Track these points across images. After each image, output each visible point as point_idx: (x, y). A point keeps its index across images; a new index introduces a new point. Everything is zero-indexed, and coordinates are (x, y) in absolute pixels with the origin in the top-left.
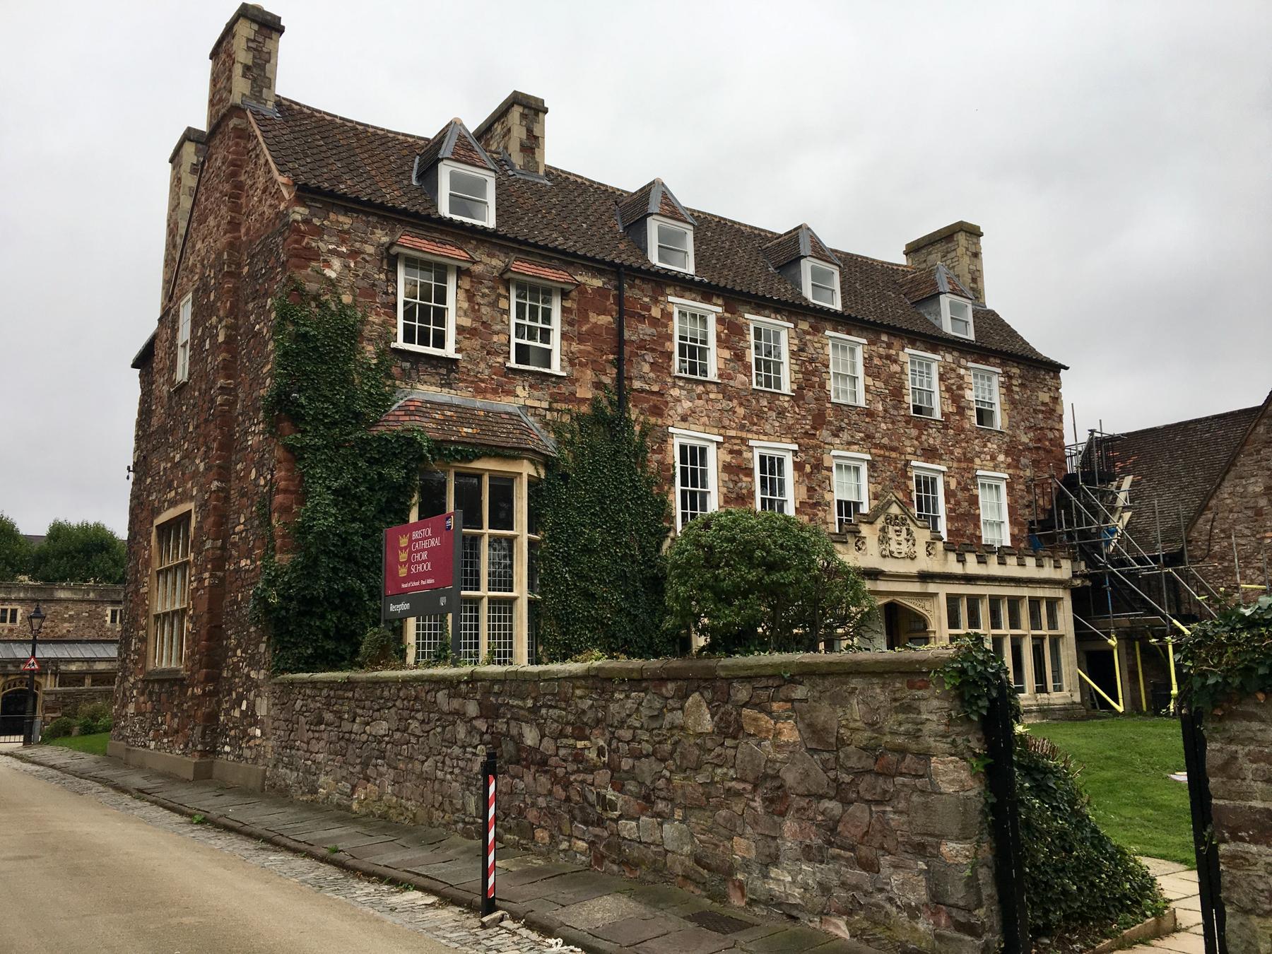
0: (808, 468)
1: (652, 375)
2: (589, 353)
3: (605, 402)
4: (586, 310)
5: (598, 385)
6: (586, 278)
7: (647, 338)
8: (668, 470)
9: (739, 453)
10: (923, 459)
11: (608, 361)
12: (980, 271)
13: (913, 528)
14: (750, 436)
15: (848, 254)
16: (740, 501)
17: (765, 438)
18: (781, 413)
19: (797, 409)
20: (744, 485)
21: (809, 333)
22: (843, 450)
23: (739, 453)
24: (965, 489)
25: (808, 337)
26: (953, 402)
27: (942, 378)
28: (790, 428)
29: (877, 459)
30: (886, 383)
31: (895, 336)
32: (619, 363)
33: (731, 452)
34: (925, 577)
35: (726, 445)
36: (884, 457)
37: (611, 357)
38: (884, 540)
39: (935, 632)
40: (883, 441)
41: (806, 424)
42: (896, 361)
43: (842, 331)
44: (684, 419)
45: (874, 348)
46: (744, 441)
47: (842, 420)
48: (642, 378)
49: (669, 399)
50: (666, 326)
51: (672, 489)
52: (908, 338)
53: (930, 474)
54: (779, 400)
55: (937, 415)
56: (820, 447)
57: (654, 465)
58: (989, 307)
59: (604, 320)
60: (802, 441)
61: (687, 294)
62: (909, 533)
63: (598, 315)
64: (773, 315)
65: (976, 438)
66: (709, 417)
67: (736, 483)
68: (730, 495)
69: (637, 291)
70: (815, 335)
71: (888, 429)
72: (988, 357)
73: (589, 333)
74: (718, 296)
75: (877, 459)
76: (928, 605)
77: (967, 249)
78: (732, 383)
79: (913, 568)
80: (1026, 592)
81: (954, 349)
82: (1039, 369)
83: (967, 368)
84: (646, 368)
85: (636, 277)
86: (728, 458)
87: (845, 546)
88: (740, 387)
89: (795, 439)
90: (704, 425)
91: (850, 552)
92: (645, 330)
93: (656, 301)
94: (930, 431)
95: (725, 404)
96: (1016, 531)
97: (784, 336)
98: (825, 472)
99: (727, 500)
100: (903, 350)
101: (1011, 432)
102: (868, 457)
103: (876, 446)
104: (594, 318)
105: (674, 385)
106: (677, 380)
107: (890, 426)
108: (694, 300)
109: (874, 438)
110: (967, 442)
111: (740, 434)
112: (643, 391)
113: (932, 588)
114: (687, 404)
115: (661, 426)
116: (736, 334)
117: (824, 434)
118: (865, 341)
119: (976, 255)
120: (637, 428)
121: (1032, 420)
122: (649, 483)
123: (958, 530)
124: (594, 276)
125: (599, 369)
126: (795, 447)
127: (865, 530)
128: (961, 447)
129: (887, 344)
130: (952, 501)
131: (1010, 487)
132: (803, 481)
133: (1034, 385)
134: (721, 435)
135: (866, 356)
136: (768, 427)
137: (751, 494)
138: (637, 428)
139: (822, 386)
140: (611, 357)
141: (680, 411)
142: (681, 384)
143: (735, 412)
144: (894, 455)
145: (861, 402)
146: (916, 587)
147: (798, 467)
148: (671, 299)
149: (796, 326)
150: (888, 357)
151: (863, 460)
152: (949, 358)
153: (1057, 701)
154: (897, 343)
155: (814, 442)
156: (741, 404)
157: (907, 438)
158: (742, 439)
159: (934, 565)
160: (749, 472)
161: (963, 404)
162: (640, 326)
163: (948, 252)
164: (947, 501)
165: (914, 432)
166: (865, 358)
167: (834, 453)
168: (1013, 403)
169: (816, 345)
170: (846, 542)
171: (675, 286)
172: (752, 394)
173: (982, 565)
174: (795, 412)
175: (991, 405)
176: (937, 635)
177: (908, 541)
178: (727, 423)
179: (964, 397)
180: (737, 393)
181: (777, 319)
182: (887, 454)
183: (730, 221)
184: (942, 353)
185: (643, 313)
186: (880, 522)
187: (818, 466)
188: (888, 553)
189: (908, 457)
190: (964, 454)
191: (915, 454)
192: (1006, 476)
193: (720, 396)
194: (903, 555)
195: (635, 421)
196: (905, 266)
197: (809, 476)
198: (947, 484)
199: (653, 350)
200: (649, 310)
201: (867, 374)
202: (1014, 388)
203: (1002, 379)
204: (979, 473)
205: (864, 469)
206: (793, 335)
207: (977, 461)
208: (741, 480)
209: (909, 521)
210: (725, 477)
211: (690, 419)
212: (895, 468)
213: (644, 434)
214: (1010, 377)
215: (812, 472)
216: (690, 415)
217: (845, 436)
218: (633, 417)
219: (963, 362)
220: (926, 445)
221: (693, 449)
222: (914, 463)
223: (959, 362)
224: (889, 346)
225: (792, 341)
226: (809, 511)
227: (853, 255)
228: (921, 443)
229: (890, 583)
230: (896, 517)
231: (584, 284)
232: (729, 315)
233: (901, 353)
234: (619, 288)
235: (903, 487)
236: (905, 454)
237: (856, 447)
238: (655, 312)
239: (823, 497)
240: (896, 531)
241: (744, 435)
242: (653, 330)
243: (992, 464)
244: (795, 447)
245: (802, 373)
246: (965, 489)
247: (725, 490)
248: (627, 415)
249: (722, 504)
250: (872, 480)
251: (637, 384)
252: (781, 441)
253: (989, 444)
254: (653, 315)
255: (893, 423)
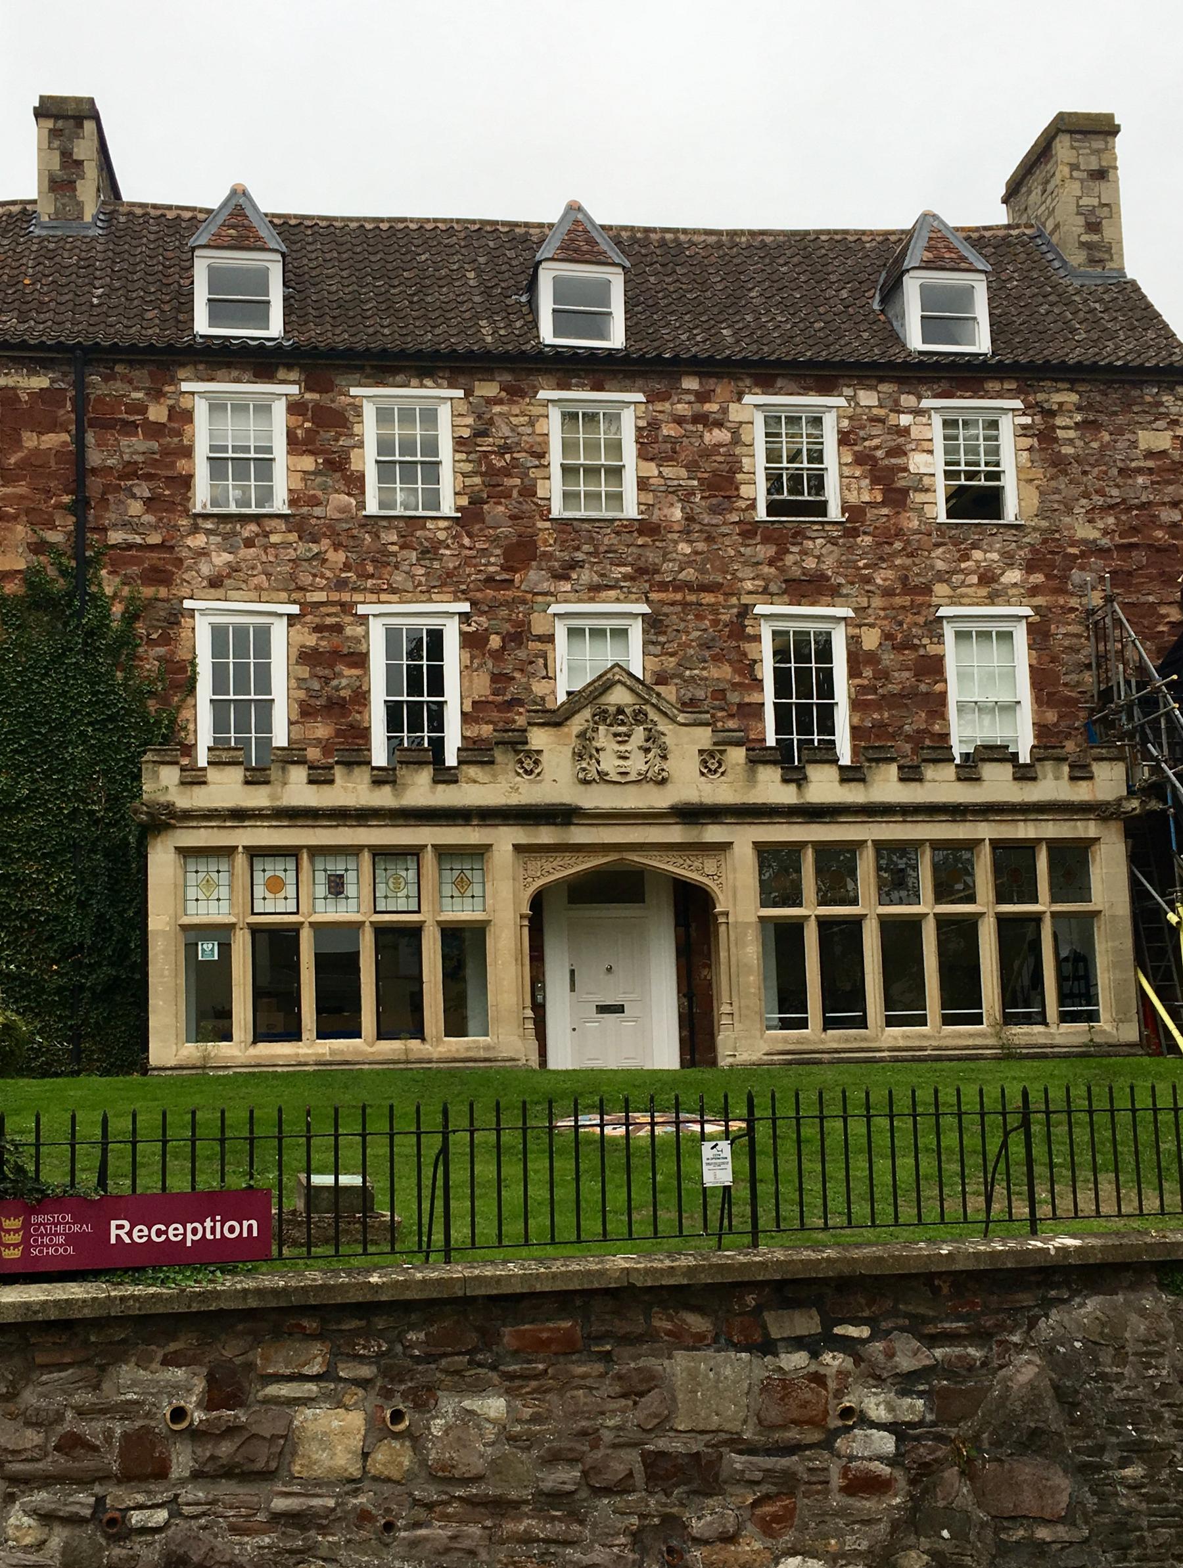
0: (495, 642)
1: (149, 518)
2: (22, 497)
3: (52, 572)
4: (17, 431)
5: (39, 547)
6: (16, 378)
7: (140, 459)
8: (183, 670)
9: (338, 628)
10: (786, 598)
11: (59, 506)
12: (1111, 208)
13: (663, 726)
14: (358, 597)
15: (794, 233)
16: (337, 710)
17: (395, 598)
18: (430, 551)
19: (466, 541)
20: (344, 682)
21: (499, 401)
22: (580, 601)
23: (338, 628)
24: (907, 645)
25: (497, 409)
26: (875, 481)
27: (844, 439)
28: (449, 575)
29: (666, 609)
30: (692, 467)
31: (719, 376)
32: (80, 507)
33: (318, 629)
34: (690, 814)
35: (309, 618)
36: (685, 604)
37: (66, 499)
38: (585, 751)
39: (727, 914)
40: (681, 576)
41: (489, 564)
42: (719, 424)
43: (581, 386)
44: (215, 583)
45: (659, 406)
46: (347, 608)
47: (578, 549)
48: (128, 525)
49: (184, 553)
50: (179, 433)
51: (190, 701)
52: (750, 375)
53: (812, 627)
54: (424, 528)
55: (834, 512)
56: (524, 602)
57: (150, 666)
58: (1130, 276)
59: (53, 440)
60: (479, 595)
61: (219, 374)
62: (652, 737)
63: (40, 433)
64: (414, 382)
65: (938, 545)
66: (268, 575)
67: (327, 680)
68: (312, 702)
69: (119, 384)
70: (512, 402)
71: (696, 553)
72: (982, 381)
73: (22, 465)
74: (289, 367)
75: (666, 609)
76: (710, 866)
77: (1074, 167)
78: (318, 511)
79: (661, 799)
80: (985, 831)
81: (882, 380)
82: (1139, 384)
83: (917, 412)
84: (135, 508)
85: (116, 362)
86: (311, 640)
87: (487, 768)
88: (337, 516)
89: (463, 592)
90: (259, 588)
91: (501, 778)
92: (136, 446)
93: (157, 394)
94: (810, 544)
95: (303, 549)
96: (1051, 716)
97: (444, 414)
98: (534, 646)
99: (305, 712)
100: (739, 400)
101: (1044, 524)
102: (645, 608)
103: (663, 587)
104: (30, 440)
105: (195, 530)
106: (200, 521)
107: (701, 546)
108: (237, 380)
109: (657, 571)
110: (911, 555)
111: (335, 596)
112: (130, 546)
113: (713, 833)
114: (222, 559)
115: (168, 600)
116: (328, 426)
117: (535, 577)
118: (640, 397)
119: (1102, 174)
120: (117, 609)
121: (1115, 492)
122: (140, 695)
123: (880, 726)
124: (32, 372)
125: (39, 519)
126: (465, 607)
127: (539, 738)
128: (892, 567)
129: (697, 394)
130: (868, 672)
131: (1039, 633)
132: (480, 666)
133: (1121, 419)
134: (294, 602)
135: (642, 423)
136: (399, 578)
137: (362, 697)
138: (117, 609)
139: (529, 491)
140: (66, 499)
141: (205, 569)
142: (210, 526)
143: (325, 561)
144: (708, 598)
145: (631, 510)
146: (675, 834)
147: (469, 641)
148: (185, 386)
149: (469, 393)
150: (701, 419)
151: (635, 616)
152: (868, 398)
153: (1058, 1040)
154: (722, 389)
155: (509, 594)
156: (337, 546)
157: (745, 564)
158: (342, 605)
159: (721, 792)
160: (361, 660)
161: (901, 484)
162: (124, 441)
163: (1047, 182)
164: (853, 672)
165: (765, 551)
166: (639, 429)
167: (554, 608)
168: (1054, 464)
169: (515, 421)
170: (492, 762)
171: (195, 364)
172: (362, 526)
173: (913, 785)
174: (463, 546)
175: (996, 476)
176: (731, 919)
177: (647, 750)
178: (305, 579)
179: (906, 469)
180: (329, 527)
181: (422, 386)
182: (692, 598)
183: (504, 223)
184: (848, 391)
185: (132, 418)
186: (578, 723)
187: (519, 635)
188: (593, 774)
189: (746, 599)
190: (904, 580)
191: (765, 591)
192: (1028, 611)
193: (293, 537)
194: (633, 777)
195: (115, 596)
196: (1008, 227)
197: (497, 655)
198: (853, 642)
199: (149, 477)
200: (143, 410)
201: (643, 455)
202: (1060, 433)
203: (1027, 420)
204: (943, 612)
205: (1021, 635)
206: (463, 408)
207: (941, 589)
208: (339, 675)
209: (653, 715)
210: (304, 672)
211: (227, 582)
212: (715, 622)
213: (131, 617)
214: (1049, 414)
215: (503, 648)
216: (229, 576)
217: (586, 576)
218: (109, 591)
219: (908, 400)
220: (796, 572)
221: (241, 631)
222: (760, 609)
223: (897, 402)
224: (703, 397)
225: (459, 421)
226: (495, 715)
227: (807, 233)
228: (781, 570)
229: (594, 829)
230: (620, 711)
231: (14, 389)
232: (316, 396)
233: (733, 407)
234: (80, 385)
235: (734, 656)
236: (738, 595)
237: (612, 593)
238: (157, 413)
239: (528, 689)
240: (616, 735)
241: (346, 597)
242: (155, 446)
243: (983, 592)
244: (465, 607)
245: (482, 474)
246: (907, 645)
247: (301, 694)
248: (94, 589)
249: (294, 718)
250: (651, 648)
251: (116, 537)
252: (430, 600)
253: (977, 555)
254: (152, 418)
255: (710, 539)
